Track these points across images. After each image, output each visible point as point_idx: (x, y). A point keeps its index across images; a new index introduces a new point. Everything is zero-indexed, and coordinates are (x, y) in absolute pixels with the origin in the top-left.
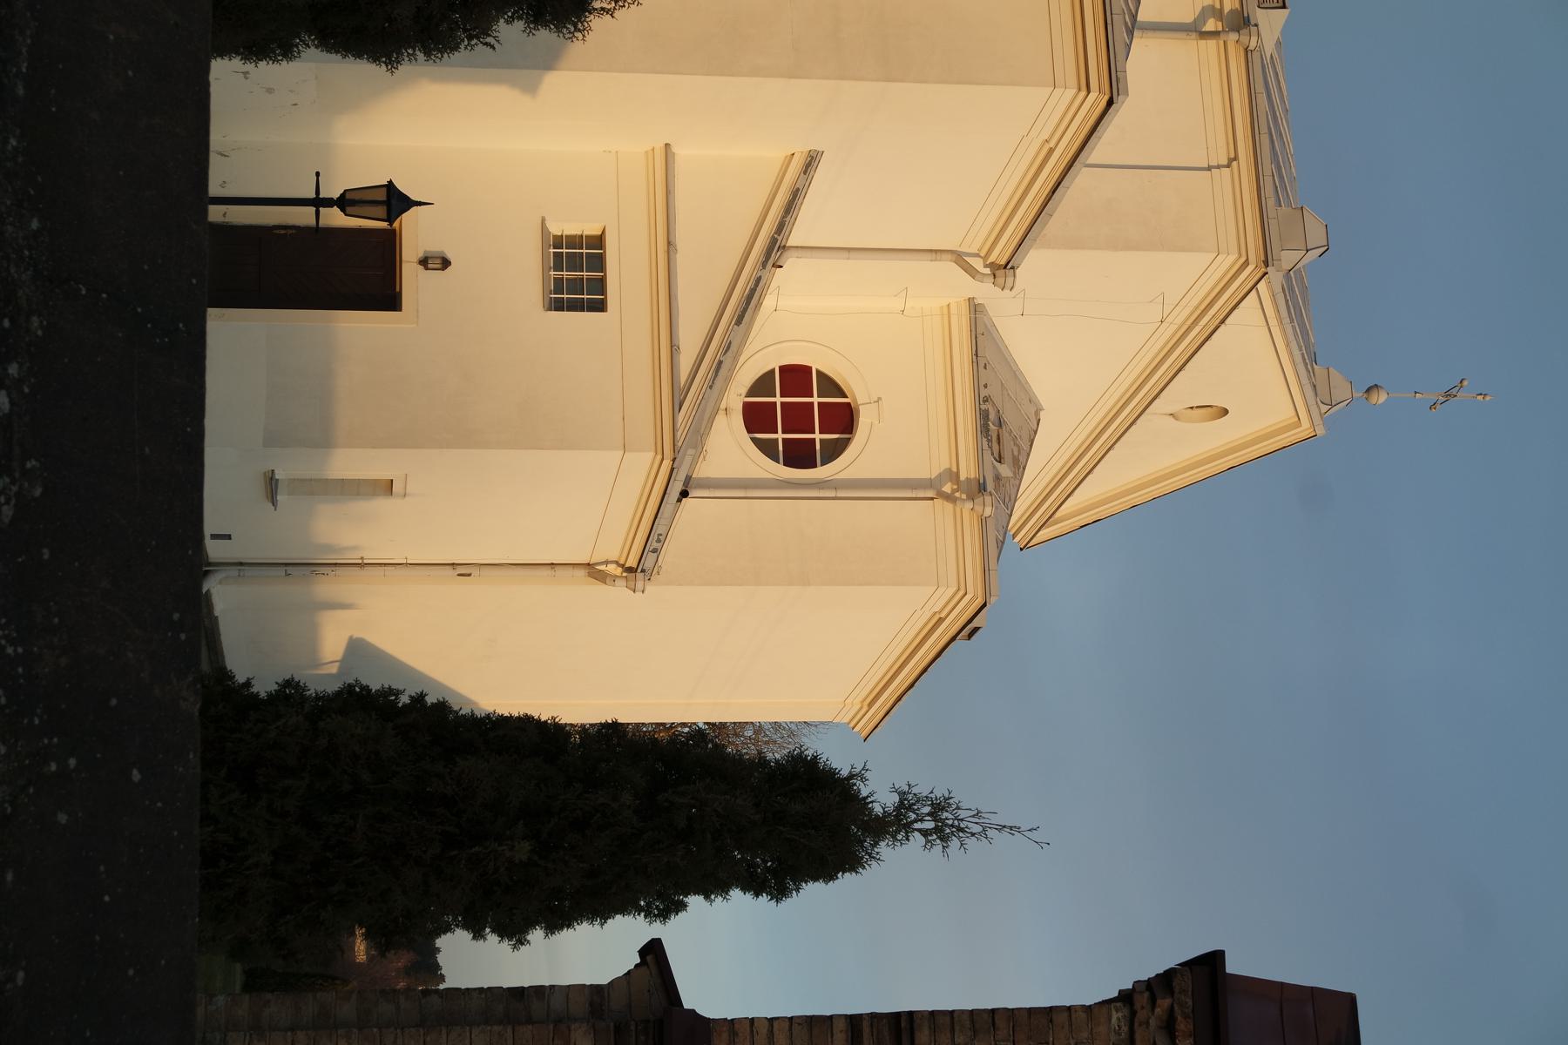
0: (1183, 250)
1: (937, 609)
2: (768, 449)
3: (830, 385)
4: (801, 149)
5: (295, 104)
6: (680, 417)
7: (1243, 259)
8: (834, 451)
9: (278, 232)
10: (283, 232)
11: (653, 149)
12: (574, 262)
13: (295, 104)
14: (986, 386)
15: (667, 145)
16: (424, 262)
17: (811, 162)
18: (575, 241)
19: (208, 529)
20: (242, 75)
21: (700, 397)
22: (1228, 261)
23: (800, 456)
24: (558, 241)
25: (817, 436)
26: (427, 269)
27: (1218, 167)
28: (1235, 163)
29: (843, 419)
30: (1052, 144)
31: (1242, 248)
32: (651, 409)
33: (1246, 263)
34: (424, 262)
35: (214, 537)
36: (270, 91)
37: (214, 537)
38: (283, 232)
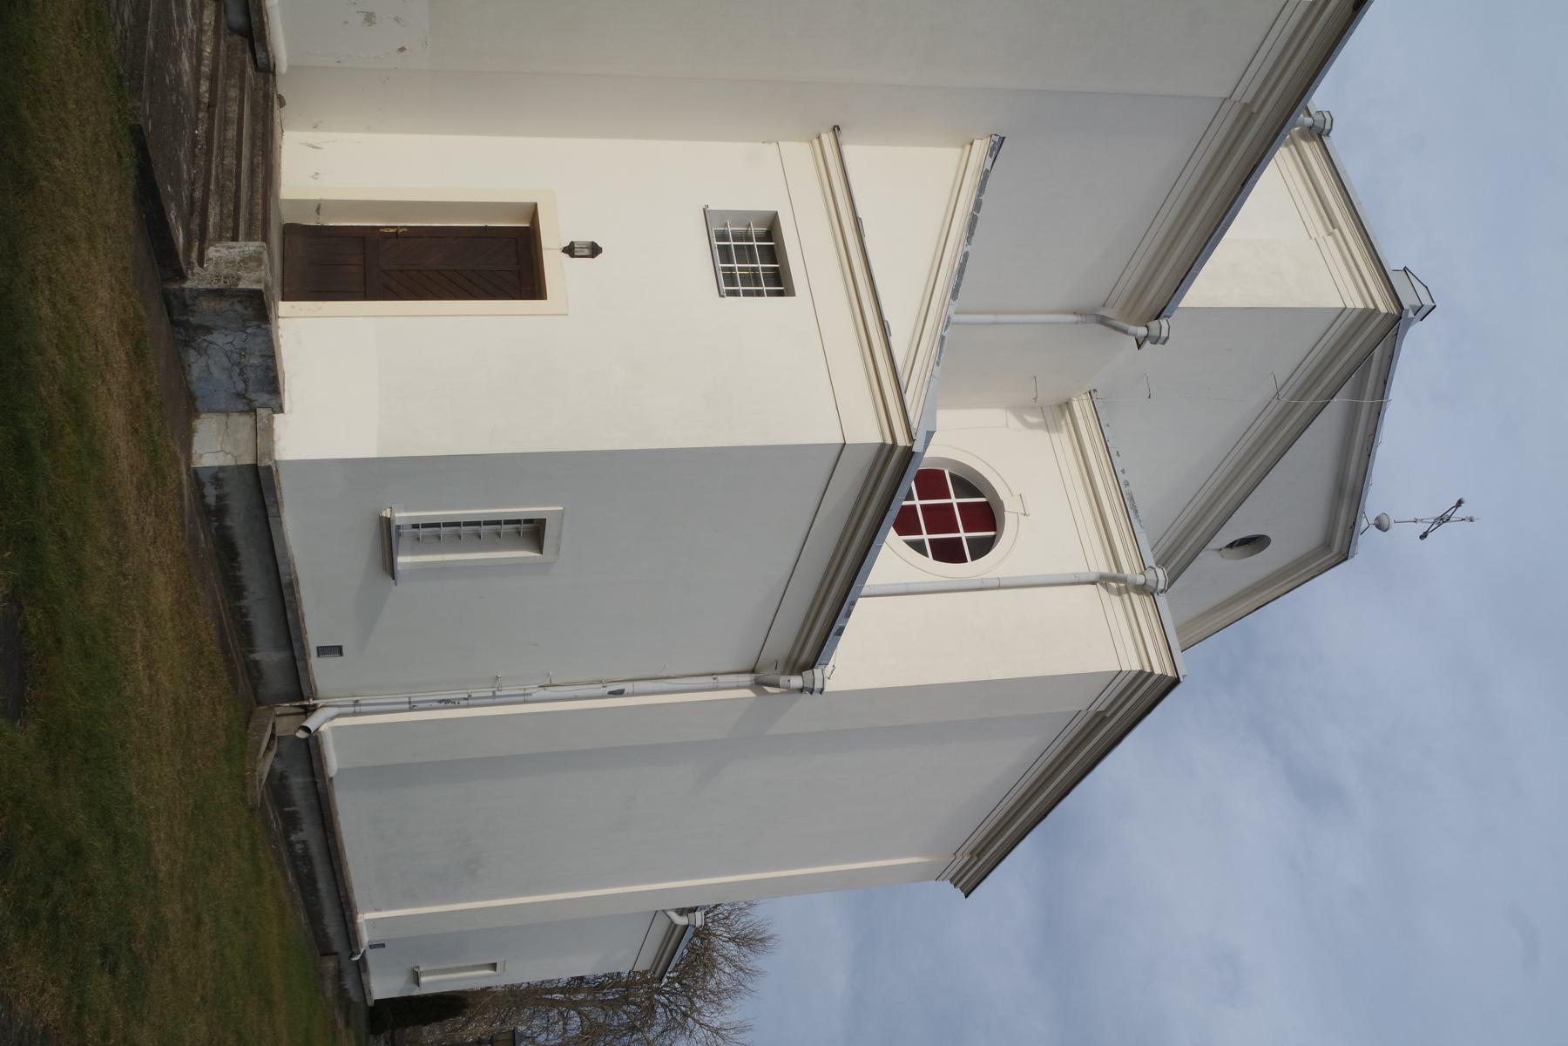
1: (1102, 708)
2: (918, 547)
3: (966, 485)
5: (402, 49)
6: (908, 398)
8: (982, 548)
10: (392, 231)
12: (746, 254)
13: (402, 49)
14: (1123, 471)
16: (570, 250)
19: (314, 638)
21: (929, 374)
23: (948, 552)
25: (963, 535)
26: (572, 256)
29: (986, 517)
30: (1255, 110)
32: (869, 397)
34: (570, 250)
35: (323, 651)
37: (323, 651)
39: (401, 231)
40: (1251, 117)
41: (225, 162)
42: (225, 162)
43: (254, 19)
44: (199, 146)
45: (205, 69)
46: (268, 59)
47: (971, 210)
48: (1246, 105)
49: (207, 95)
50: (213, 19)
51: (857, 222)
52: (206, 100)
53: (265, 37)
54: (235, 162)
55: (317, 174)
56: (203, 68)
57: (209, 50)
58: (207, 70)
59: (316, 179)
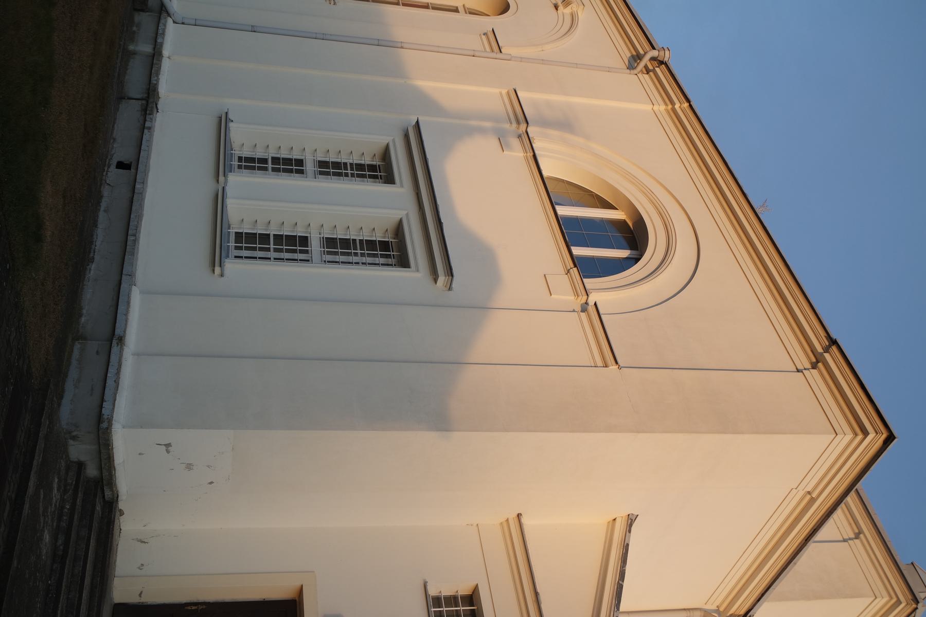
0: (852, 597)
4: (621, 513)
5: (211, 483)
7: (895, 600)
9: (189, 608)
10: (194, 608)
11: (507, 520)
13: (211, 483)
15: (519, 515)
17: (631, 521)
18: (452, 600)
20: (164, 448)
22: (882, 601)
24: (437, 601)
27: (850, 539)
28: (862, 536)
30: (814, 495)
31: (891, 592)
33: (899, 602)
36: (189, 467)
38: (194, 608)
39: (201, 607)
40: (812, 501)
41: (70, 596)
42: (70, 596)
43: (105, 473)
44: (50, 595)
45: (63, 524)
46: (113, 495)
47: (617, 580)
48: (809, 493)
49: (61, 547)
50: (75, 479)
51: (536, 594)
52: (60, 553)
53: (112, 484)
54: (77, 596)
55: (142, 565)
56: (62, 523)
57: (68, 507)
58: (64, 525)
59: (141, 569)
